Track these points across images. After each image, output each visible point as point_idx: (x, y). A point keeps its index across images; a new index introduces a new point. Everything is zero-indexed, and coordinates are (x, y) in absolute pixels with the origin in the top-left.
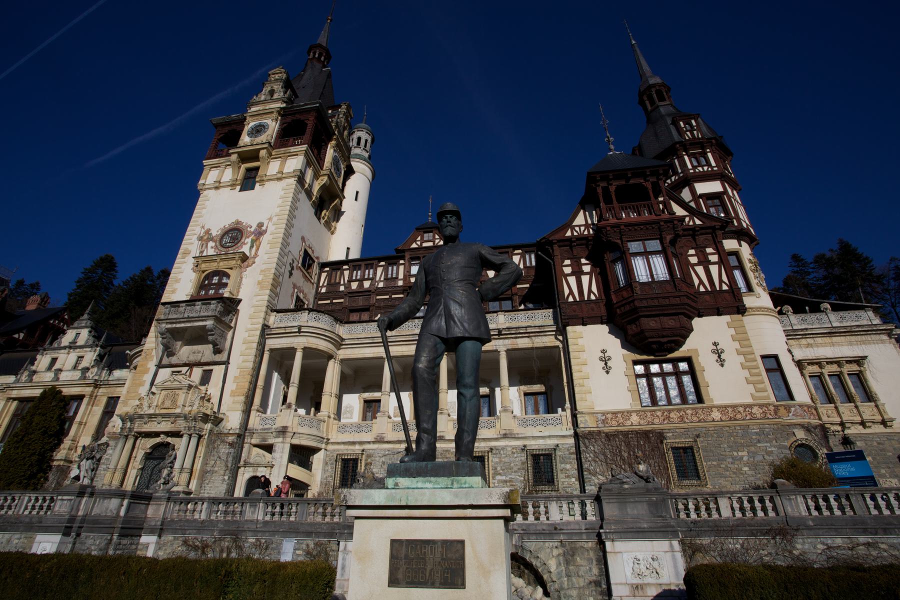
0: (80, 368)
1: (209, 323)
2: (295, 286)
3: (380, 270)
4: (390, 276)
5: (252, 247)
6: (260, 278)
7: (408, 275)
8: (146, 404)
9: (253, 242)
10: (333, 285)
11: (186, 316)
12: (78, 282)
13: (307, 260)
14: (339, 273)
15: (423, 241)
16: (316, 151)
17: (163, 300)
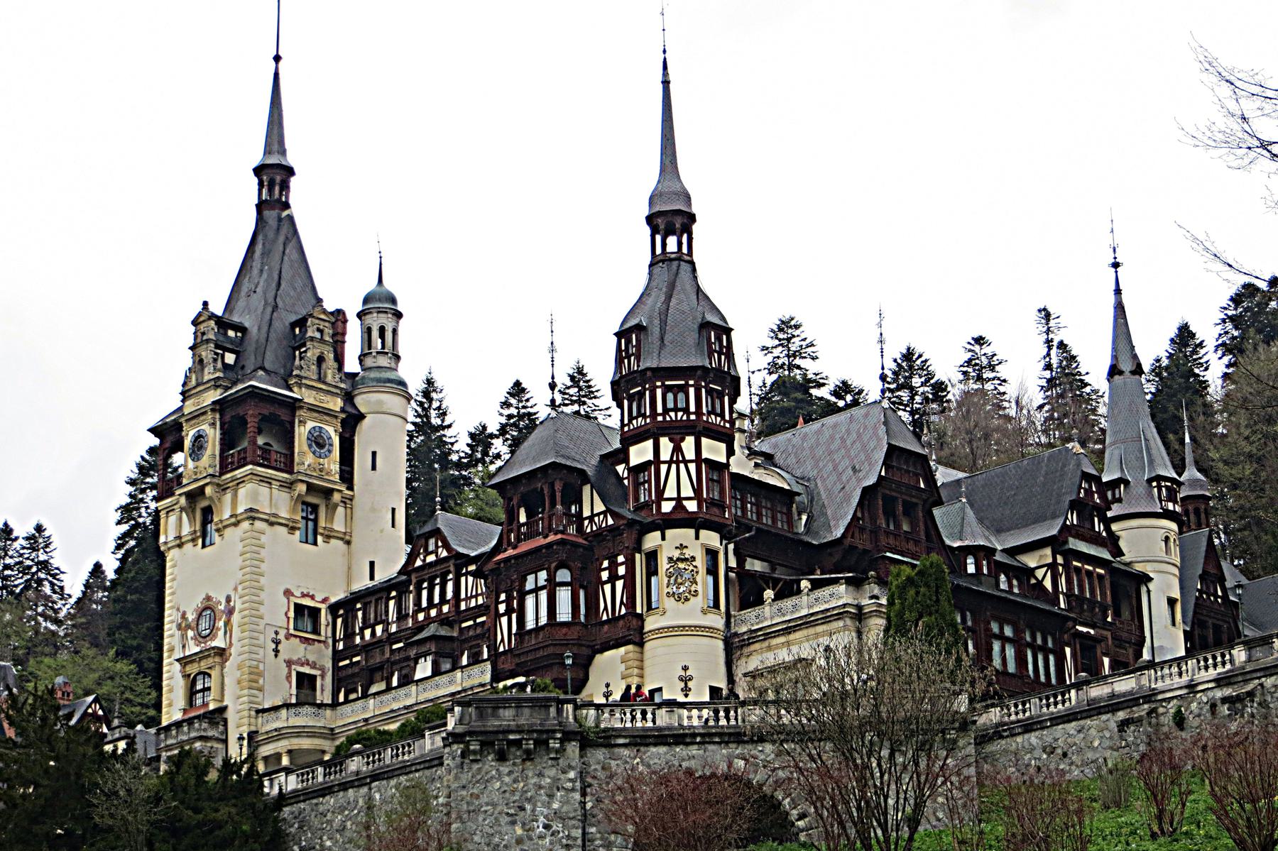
2: (289, 663)
6: (238, 674)
7: (419, 609)
10: (349, 636)
15: (427, 553)
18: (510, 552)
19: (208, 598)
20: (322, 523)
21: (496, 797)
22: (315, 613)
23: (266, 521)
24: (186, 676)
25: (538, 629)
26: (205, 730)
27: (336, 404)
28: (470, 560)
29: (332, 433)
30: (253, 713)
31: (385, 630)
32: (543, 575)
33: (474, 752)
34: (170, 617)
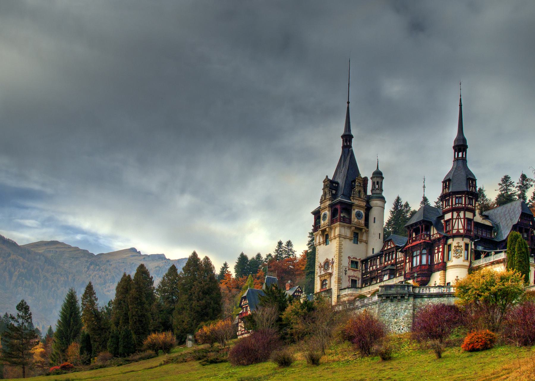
2: (349, 277)
7: (385, 261)
10: (366, 269)
12: (309, 244)
13: (354, 263)
15: (388, 246)
18: (410, 245)
19: (327, 259)
20: (359, 238)
21: (390, 311)
22: (357, 263)
24: (321, 280)
25: (416, 267)
27: (364, 204)
28: (400, 248)
29: (362, 212)
31: (376, 267)
32: (419, 252)
33: (384, 300)
34: (317, 264)
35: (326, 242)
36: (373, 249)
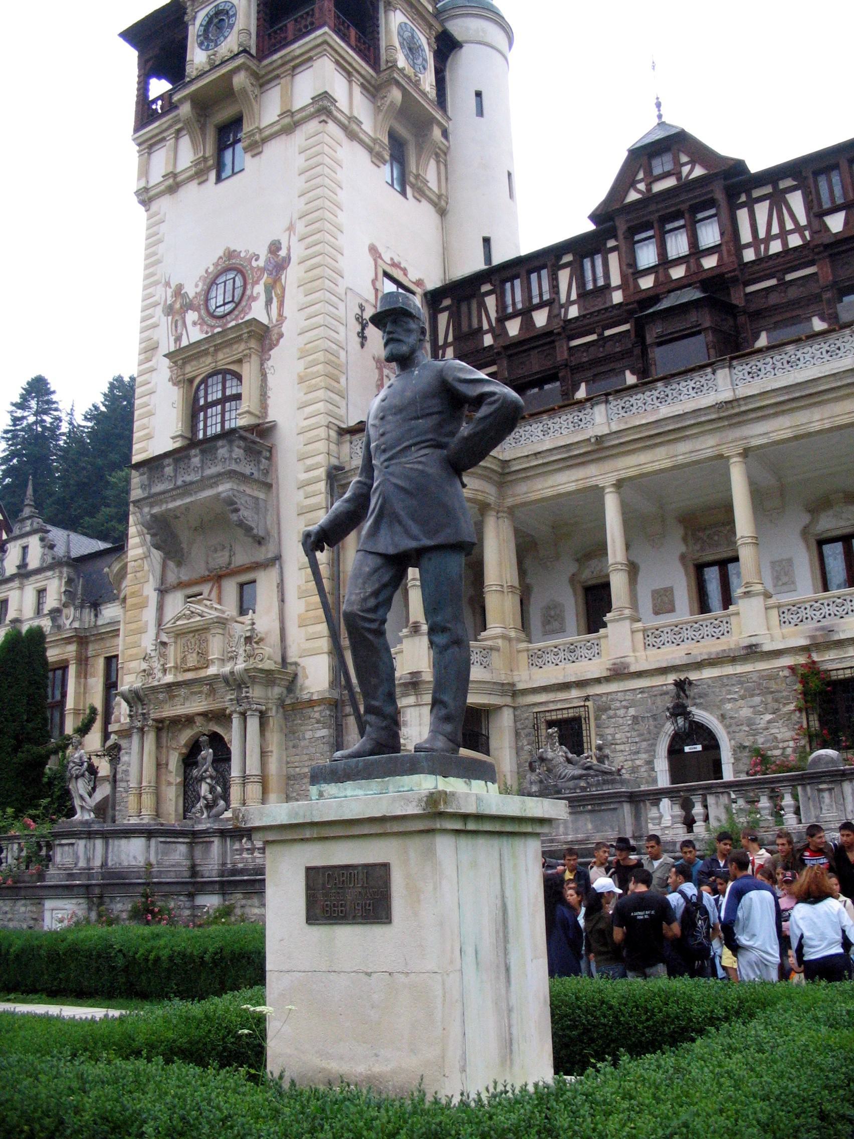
0: (46, 612)
1: (224, 488)
3: (564, 276)
4: (590, 286)
5: (269, 302)
6: (300, 366)
7: (632, 272)
8: (157, 665)
9: (269, 289)
11: (179, 483)
14: (474, 306)
15: (652, 179)
16: (353, 32)
17: (136, 459)
19: (230, 254)
20: (412, 167)
23: (344, 128)
26: (237, 461)
30: (333, 434)
35: (220, 167)
36: (487, 241)
